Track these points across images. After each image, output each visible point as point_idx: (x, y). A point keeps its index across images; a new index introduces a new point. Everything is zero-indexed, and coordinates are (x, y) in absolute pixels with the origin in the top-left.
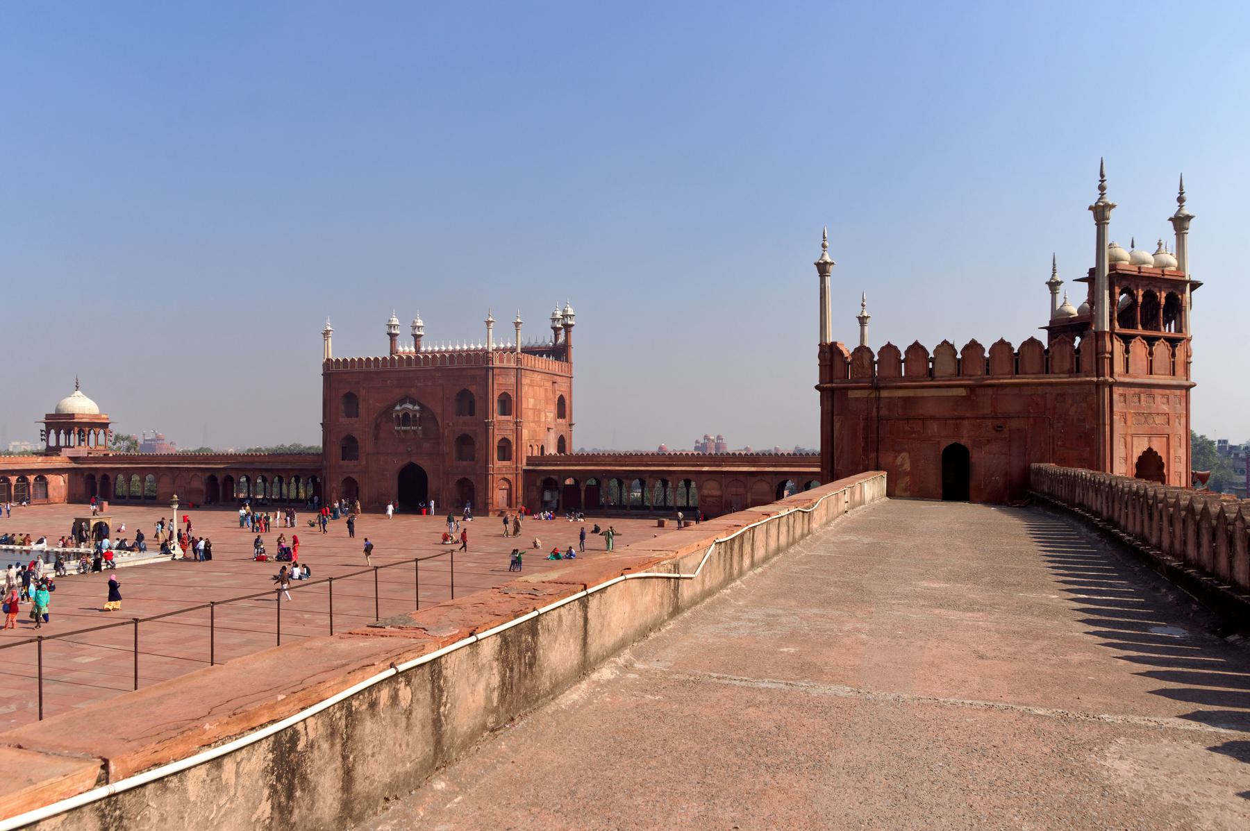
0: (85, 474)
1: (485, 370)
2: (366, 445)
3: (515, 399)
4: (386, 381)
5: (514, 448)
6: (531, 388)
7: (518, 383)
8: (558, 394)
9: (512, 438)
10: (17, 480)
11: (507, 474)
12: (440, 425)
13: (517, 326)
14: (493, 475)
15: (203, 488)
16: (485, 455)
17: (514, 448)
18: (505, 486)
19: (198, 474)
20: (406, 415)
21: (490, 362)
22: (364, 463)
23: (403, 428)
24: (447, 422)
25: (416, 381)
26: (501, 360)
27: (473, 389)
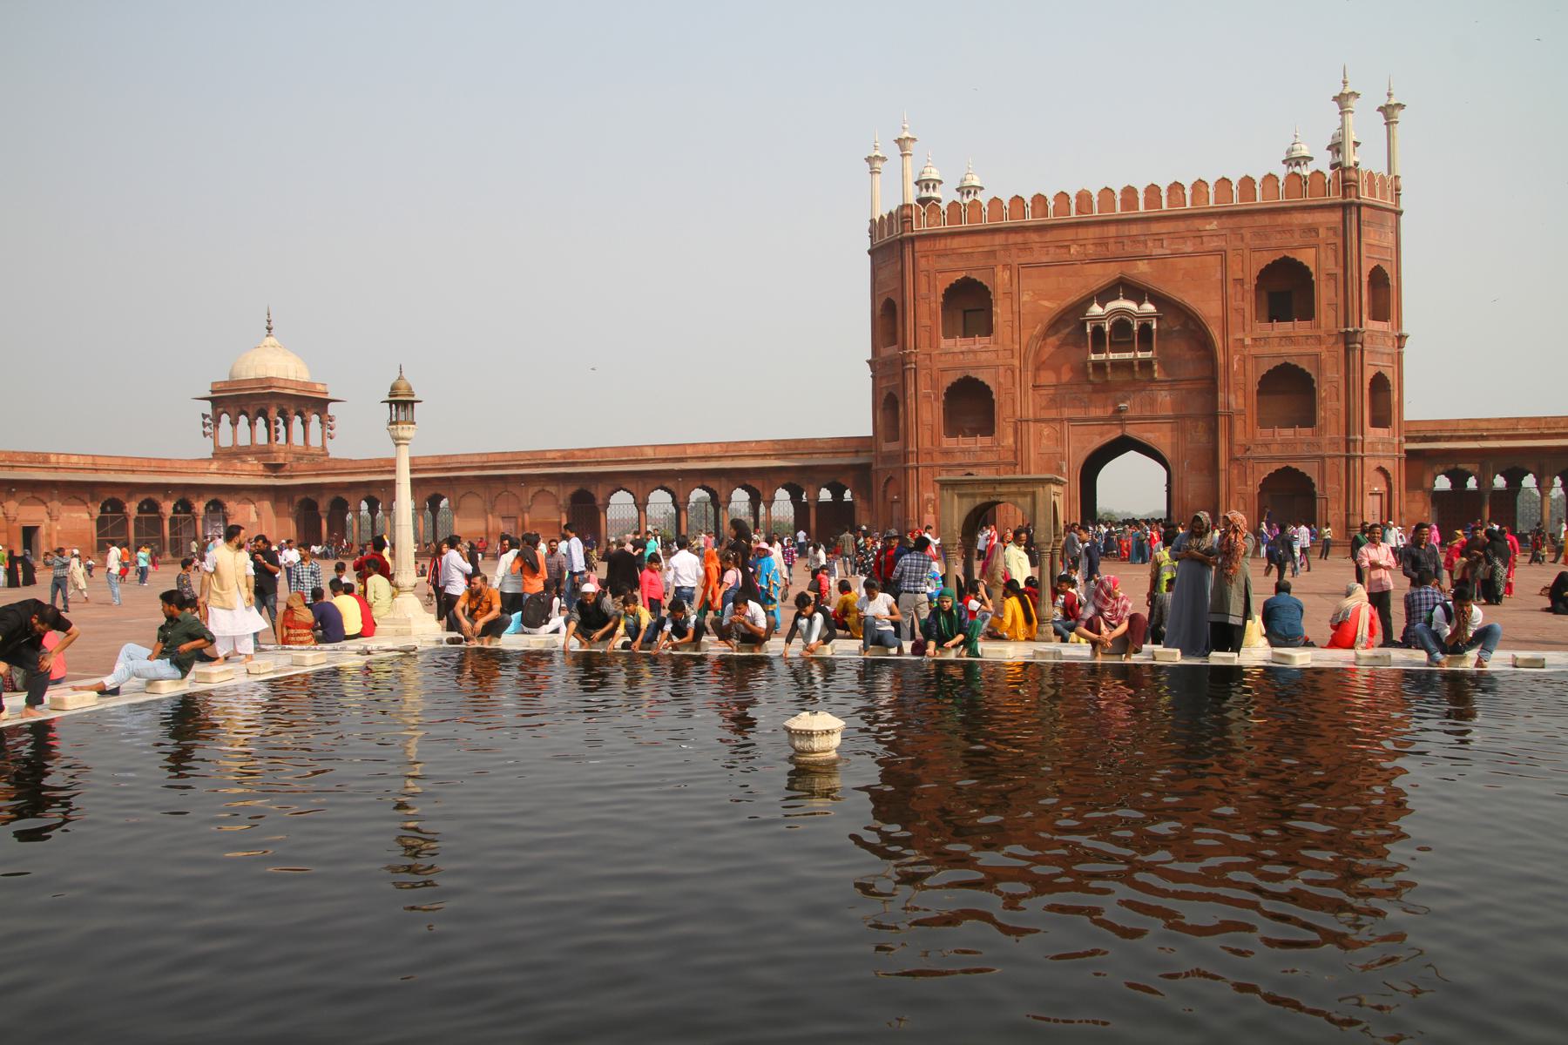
3: (1395, 284)
4: (1068, 247)
9: (1390, 375)
11: (1384, 457)
12: (1219, 344)
13: (1387, 117)
14: (1362, 458)
16: (1343, 409)
17: (1395, 397)
19: (547, 488)
20: (1122, 325)
21: (1353, 192)
22: (1011, 440)
23: (1112, 356)
24: (1239, 336)
25: (1150, 244)
27: (1306, 257)
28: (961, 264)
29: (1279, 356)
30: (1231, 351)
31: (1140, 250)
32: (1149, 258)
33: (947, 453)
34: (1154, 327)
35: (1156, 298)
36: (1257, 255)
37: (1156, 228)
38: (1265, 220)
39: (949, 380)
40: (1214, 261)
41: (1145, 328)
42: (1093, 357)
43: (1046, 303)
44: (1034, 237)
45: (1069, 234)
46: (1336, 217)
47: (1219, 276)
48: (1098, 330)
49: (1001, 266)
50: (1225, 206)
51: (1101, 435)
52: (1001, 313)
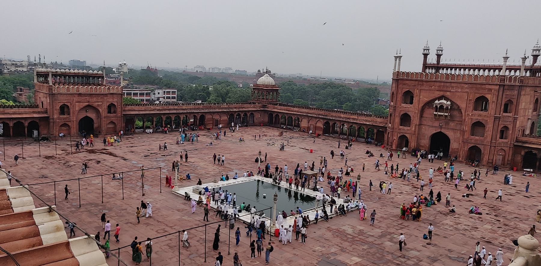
0: (269, 113)
1: (498, 86)
2: (415, 120)
5: (511, 132)
6: (524, 96)
7: (519, 95)
8: (536, 97)
10: (243, 115)
15: (322, 127)
18: (504, 154)
22: (414, 129)
23: (439, 113)
26: (510, 81)
27: (489, 97)
28: (408, 87)
29: (478, 119)
30: (466, 117)
31: (449, 89)
32: (450, 91)
33: (400, 129)
34: (449, 108)
35: (451, 101)
36: (476, 94)
37: (453, 85)
38: (479, 86)
39: (402, 113)
40: (466, 94)
41: (447, 107)
42: (435, 113)
43: (425, 99)
44: (425, 83)
45: (432, 83)
46: (497, 87)
47: (466, 98)
48: (436, 106)
49: (416, 89)
50: (470, 81)
51: (435, 130)
52: (415, 100)
